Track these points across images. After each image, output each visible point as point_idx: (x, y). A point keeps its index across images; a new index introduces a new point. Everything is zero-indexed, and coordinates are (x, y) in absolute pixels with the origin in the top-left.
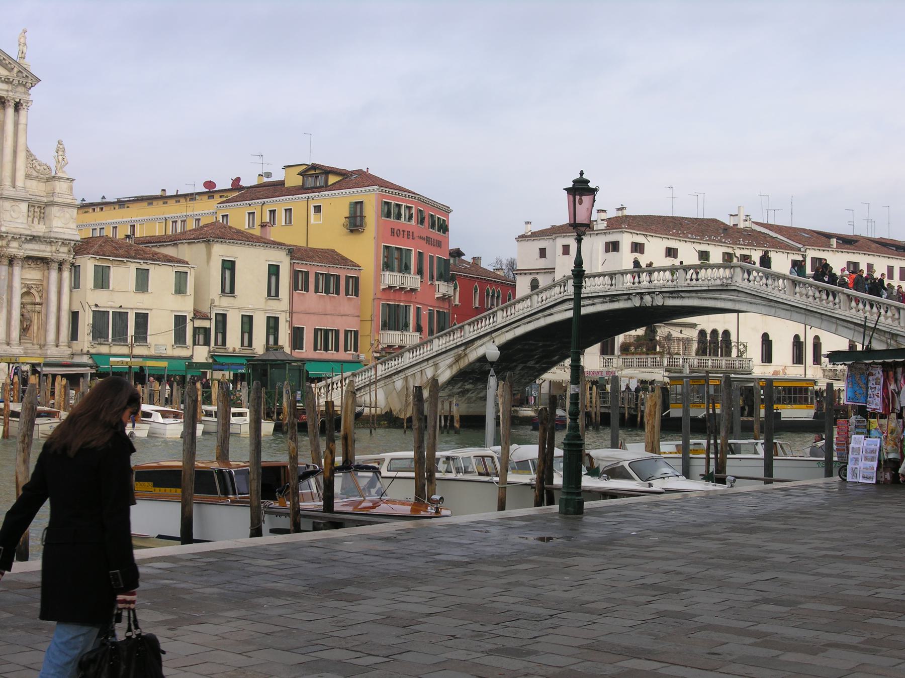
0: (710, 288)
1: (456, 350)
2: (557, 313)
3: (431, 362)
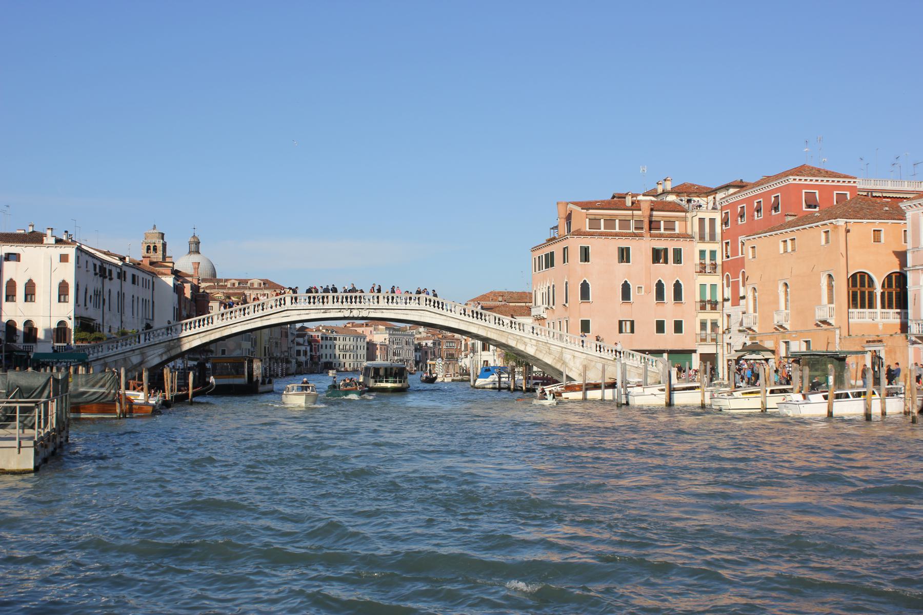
1: (168, 343)
3: (137, 352)
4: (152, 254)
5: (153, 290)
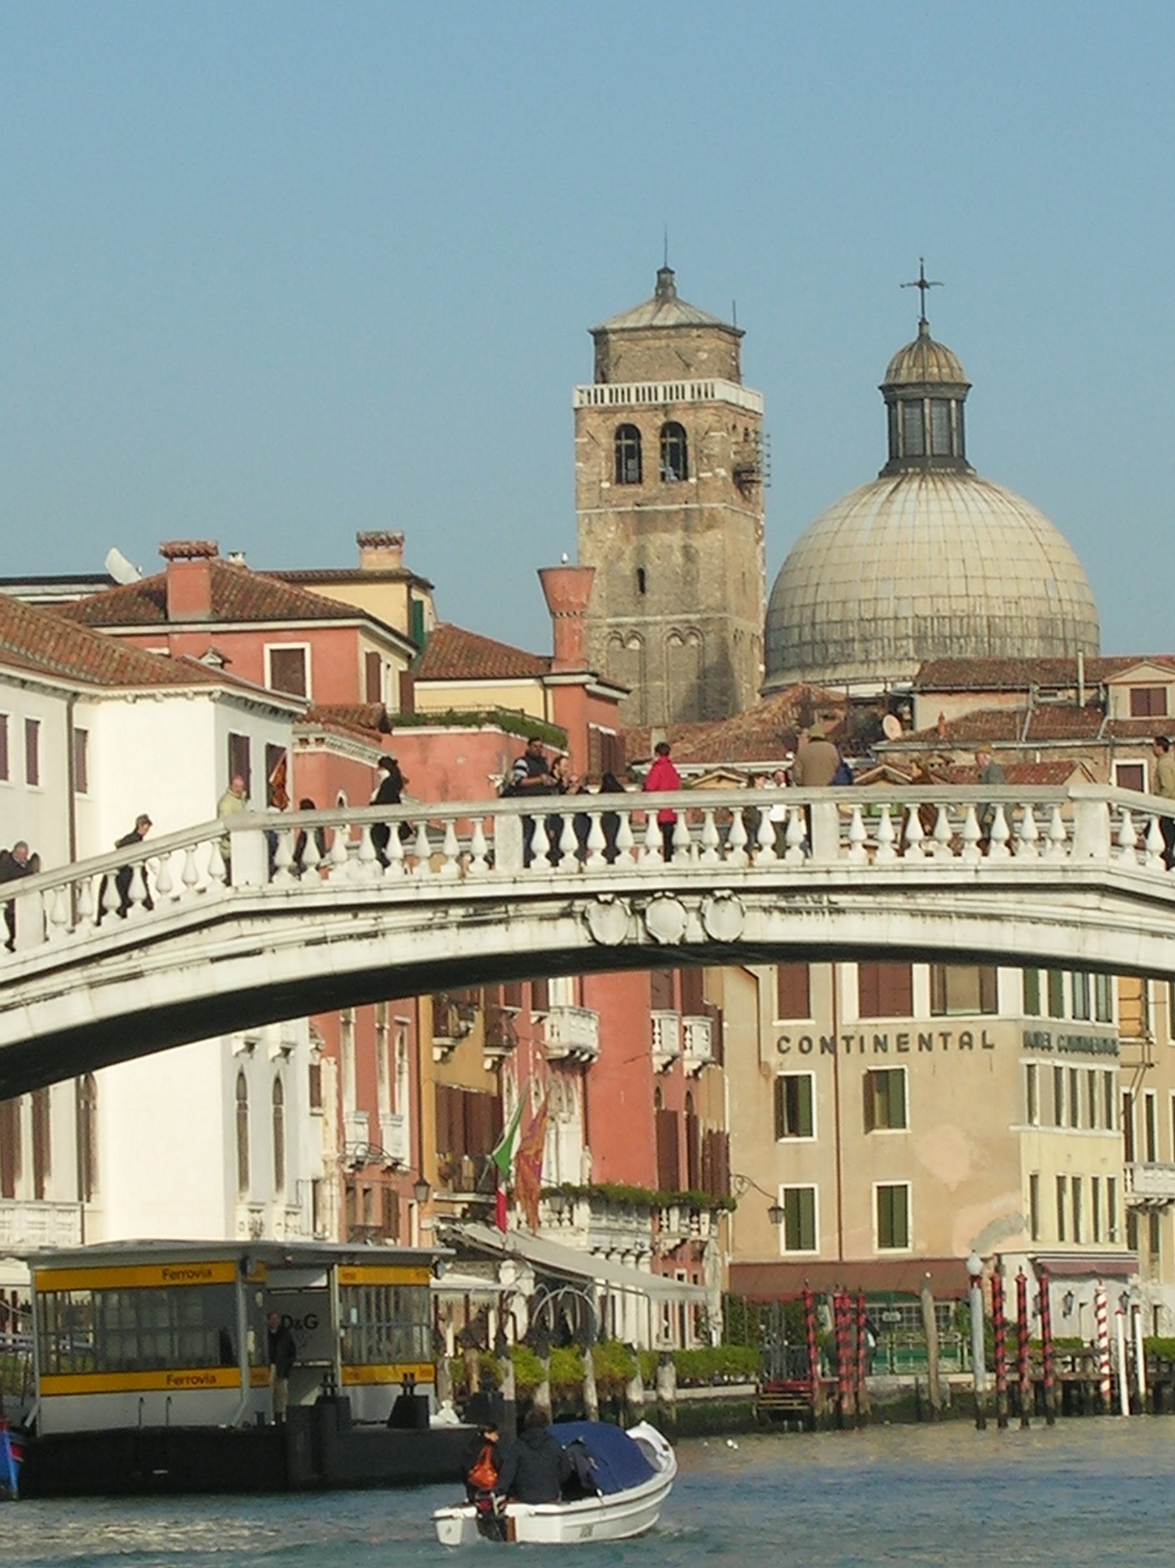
0: (985, 878)
2: (163, 969)
4: (651, 485)
5: (78, 780)
